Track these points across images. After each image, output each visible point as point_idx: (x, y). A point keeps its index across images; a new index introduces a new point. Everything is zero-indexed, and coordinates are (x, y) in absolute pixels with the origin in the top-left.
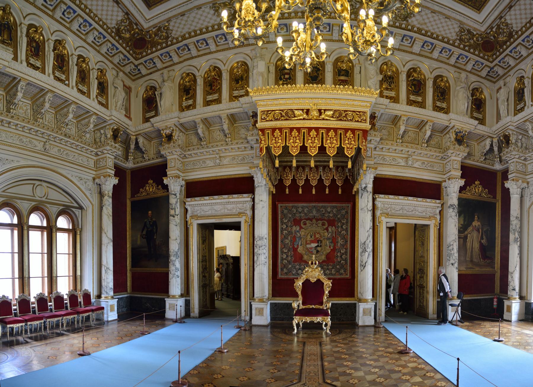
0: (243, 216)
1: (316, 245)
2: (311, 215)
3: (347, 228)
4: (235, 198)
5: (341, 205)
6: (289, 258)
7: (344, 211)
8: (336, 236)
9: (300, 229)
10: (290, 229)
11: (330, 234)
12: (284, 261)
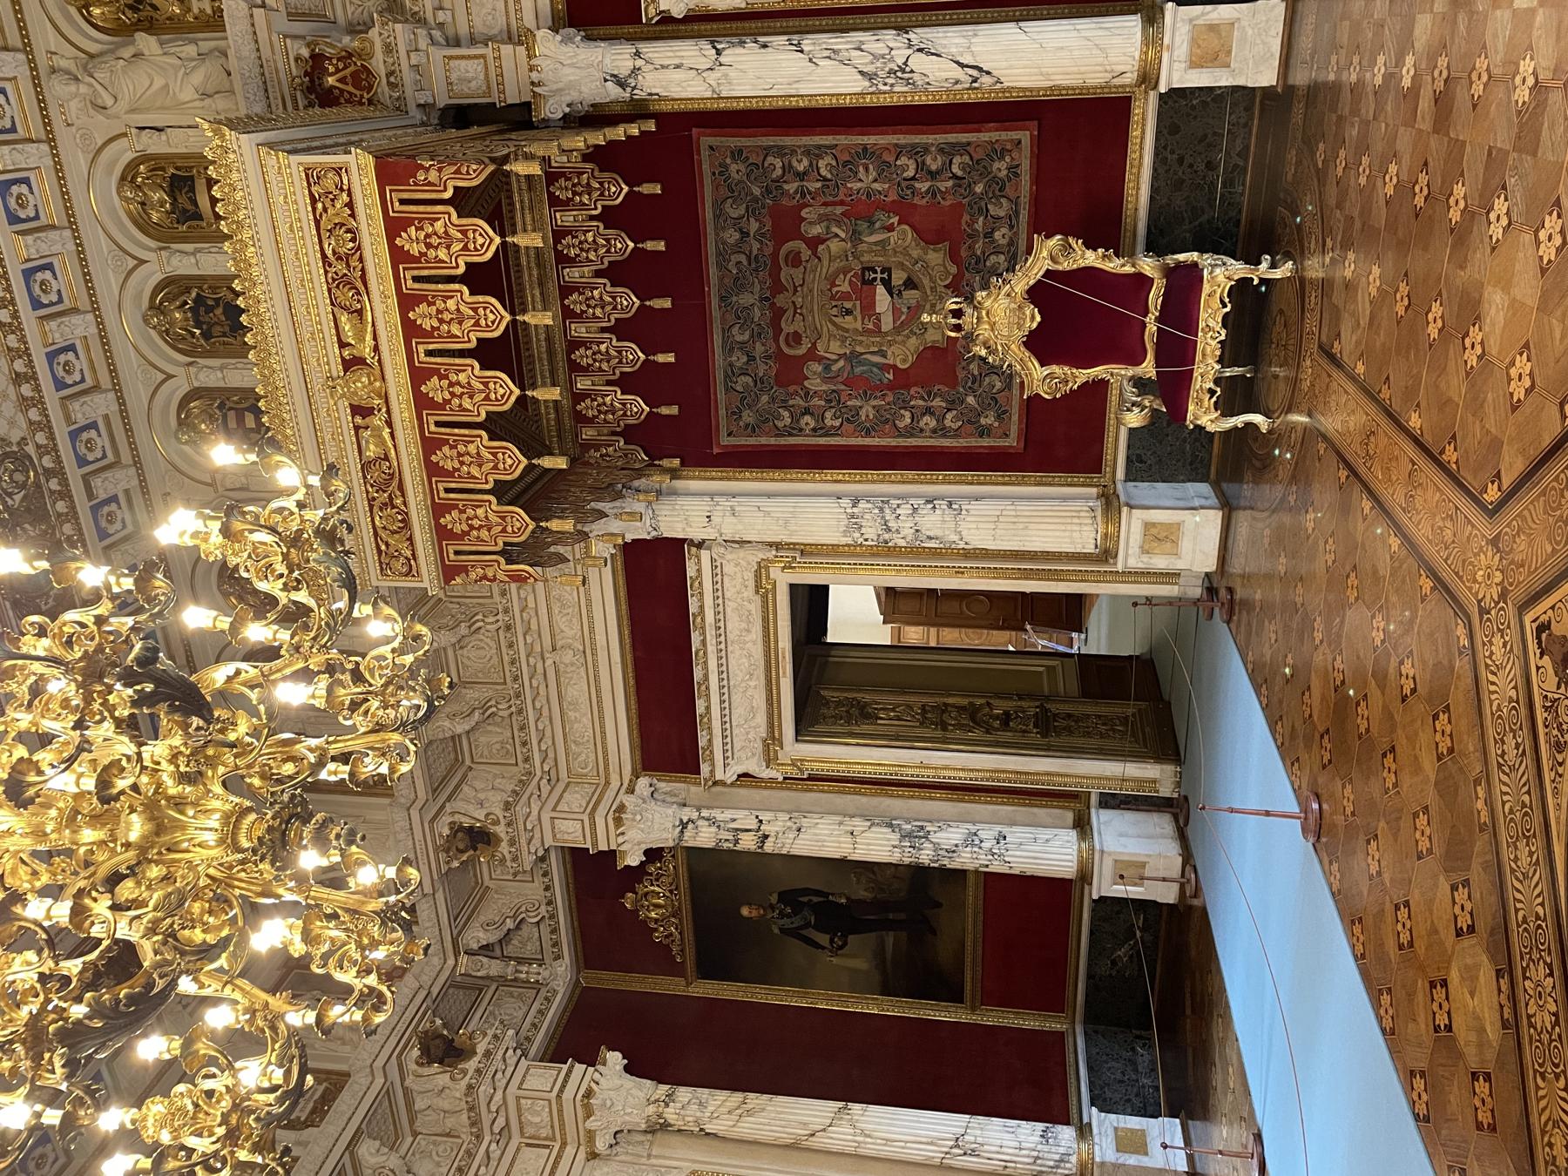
0: (768, 577)
1: (881, 290)
2: (757, 313)
3: (807, 153)
4: (702, 607)
5: (707, 181)
6: (937, 402)
7: (734, 167)
8: (842, 203)
9: (820, 359)
10: (816, 401)
11: (835, 230)
12: (948, 423)
